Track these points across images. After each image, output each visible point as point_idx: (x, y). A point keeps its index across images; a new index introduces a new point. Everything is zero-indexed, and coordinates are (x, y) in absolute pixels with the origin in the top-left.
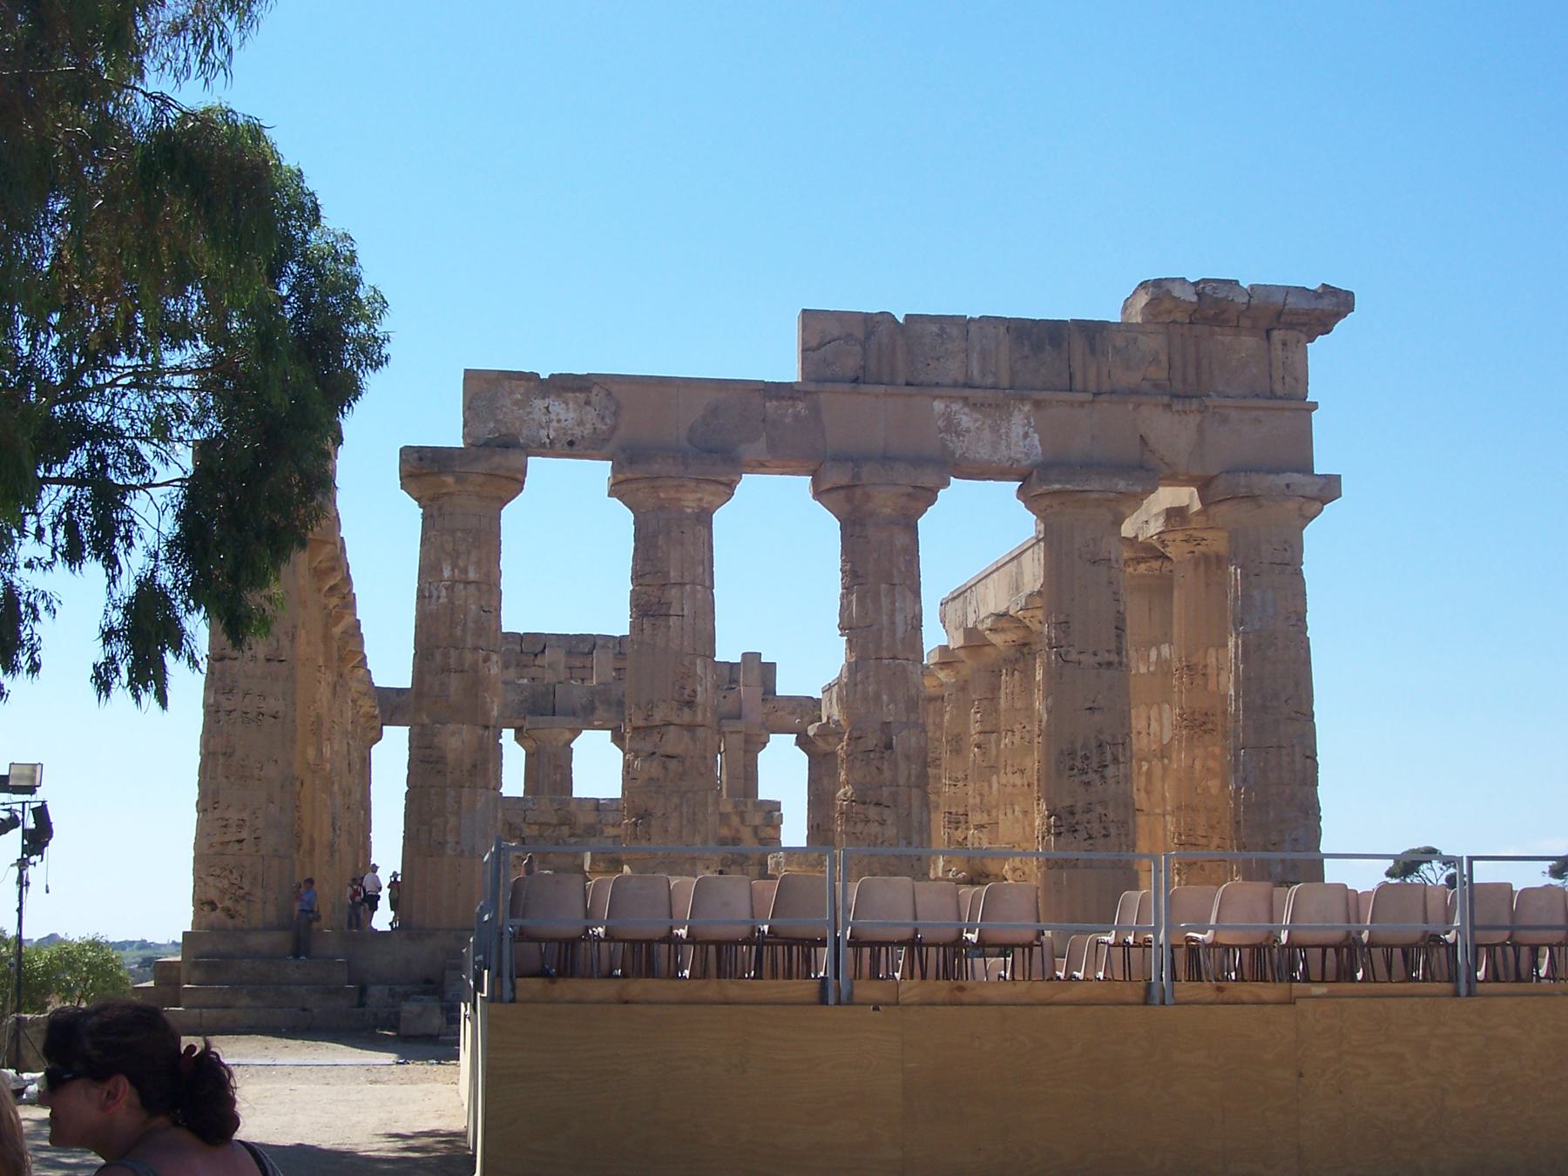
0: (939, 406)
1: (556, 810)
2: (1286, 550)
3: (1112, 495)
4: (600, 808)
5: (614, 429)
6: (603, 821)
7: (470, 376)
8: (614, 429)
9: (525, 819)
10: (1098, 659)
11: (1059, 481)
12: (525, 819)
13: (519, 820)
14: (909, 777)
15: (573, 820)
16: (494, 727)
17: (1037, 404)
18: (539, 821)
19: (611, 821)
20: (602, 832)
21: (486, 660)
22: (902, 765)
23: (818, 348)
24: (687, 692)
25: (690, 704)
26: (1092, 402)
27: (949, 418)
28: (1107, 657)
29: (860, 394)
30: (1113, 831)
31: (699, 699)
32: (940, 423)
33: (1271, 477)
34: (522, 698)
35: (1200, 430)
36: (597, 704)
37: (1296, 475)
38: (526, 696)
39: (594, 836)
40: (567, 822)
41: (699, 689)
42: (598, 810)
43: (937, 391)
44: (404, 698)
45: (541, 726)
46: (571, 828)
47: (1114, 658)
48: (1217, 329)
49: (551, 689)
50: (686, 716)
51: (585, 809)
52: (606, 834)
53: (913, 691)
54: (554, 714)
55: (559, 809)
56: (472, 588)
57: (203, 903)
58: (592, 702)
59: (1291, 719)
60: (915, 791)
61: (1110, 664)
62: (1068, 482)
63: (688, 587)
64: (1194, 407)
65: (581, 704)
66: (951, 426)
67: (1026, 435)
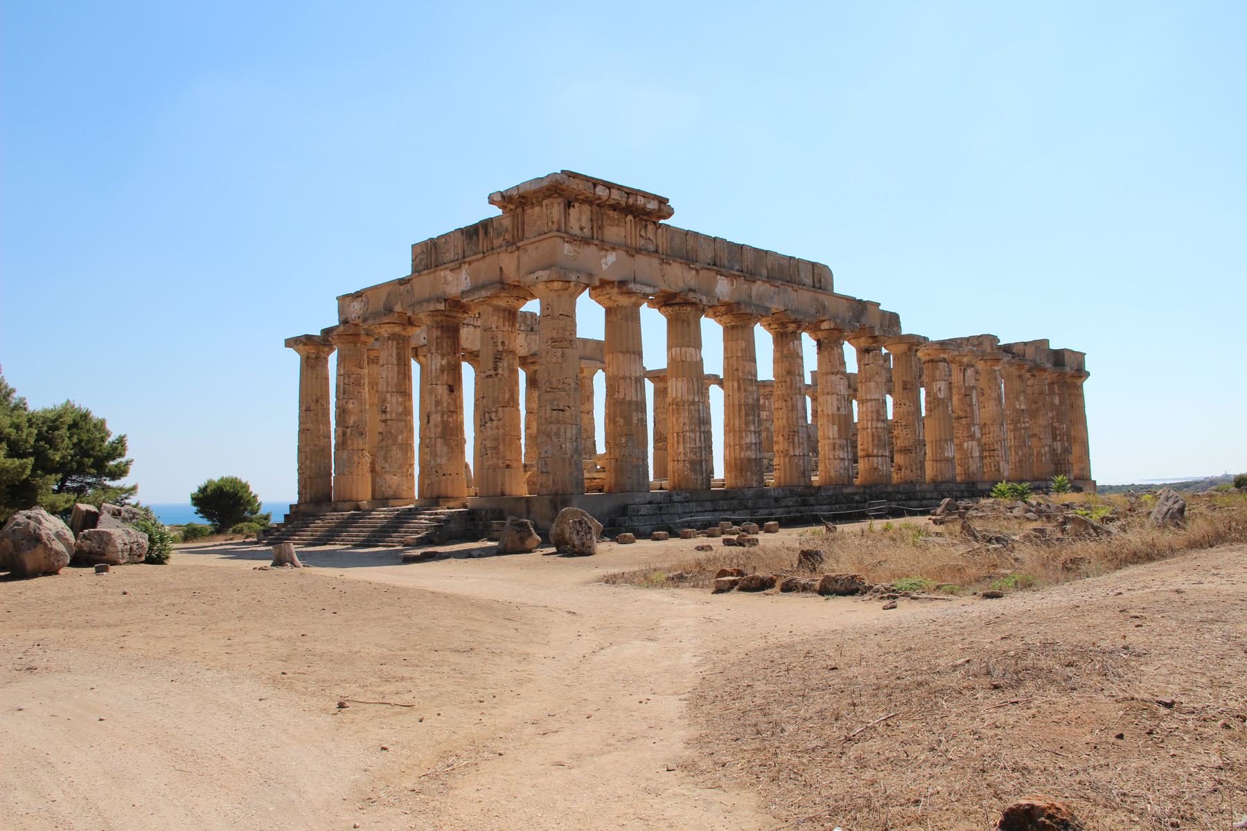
0: (442, 273)
2: (548, 309)
3: (482, 299)
5: (367, 309)
7: (338, 298)
8: (367, 309)
10: (486, 374)
11: (466, 298)
14: (435, 434)
16: (352, 427)
17: (470, 263)
21: (346, 403)
22: (433, 429)
23: (416, 258)
24: (384, 407)
25: (384, 412)
26: (484, 257)
27: (445, 278)
28: (490, 373)
29: (423, 275)
30: (489, 452)
31: (388, 410)
32: (443, 281)
33: (532, 275)
35: (519, 260)
37: (540, 272)
41: (388, 406)
43: (443, 267)
47: (492, 372)
48: (526, 208)
50: (384, 417)
53: (439, 397)
56: (342, 377)
57: (300, 493)
59: (546, 392)
60: (439, 440)
61: (491, 375)
62: (468, 297)
63: (385, 366)
64: (514, 248)
66: (446, 282)
67: (466, 279)
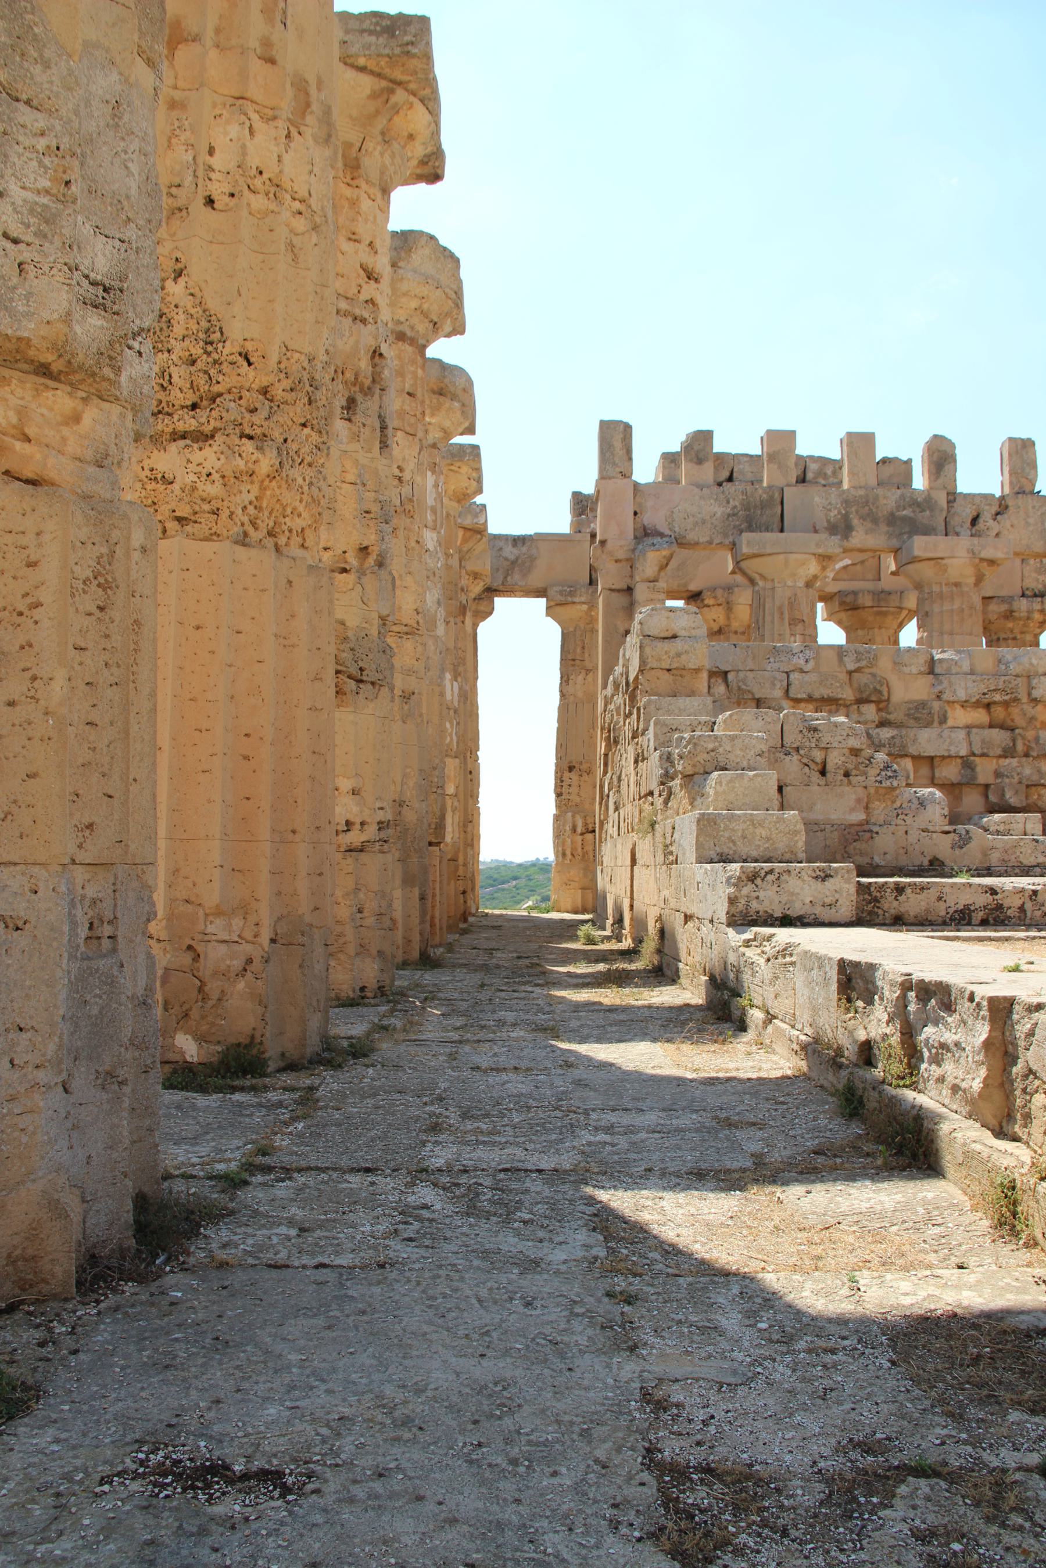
1: (850, 673)
4: (937, 670)
6: (945, 697)
9: (787, 691)
12: (787, 691)
13: (778, 693)
15: (886, 694)
18: (817, 695)
19: (962, 695)
20: (943, 720)
34: (728, 511)
36: (855, 522)
38: (735, 507)
39: (928, 724)
40: (873, 698)
42: (931, 672)
44: (524, 549)
45: (768, 551)
46: (879, 710)
49: (777, 496)
51: (906, 670)
52: (950, 722)
54: (782, 531)
55: (858, 670)
58: (846, 518)
65: (828, 521)
